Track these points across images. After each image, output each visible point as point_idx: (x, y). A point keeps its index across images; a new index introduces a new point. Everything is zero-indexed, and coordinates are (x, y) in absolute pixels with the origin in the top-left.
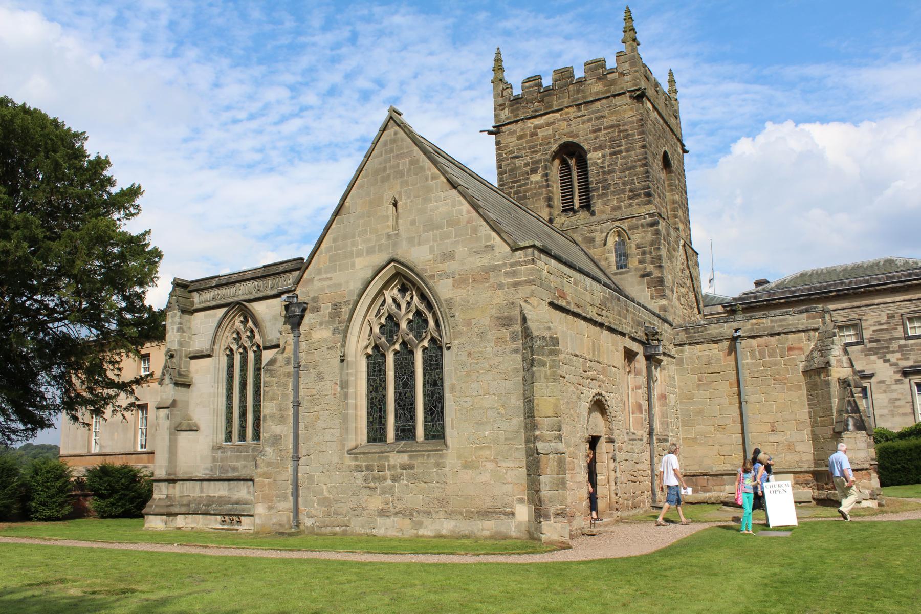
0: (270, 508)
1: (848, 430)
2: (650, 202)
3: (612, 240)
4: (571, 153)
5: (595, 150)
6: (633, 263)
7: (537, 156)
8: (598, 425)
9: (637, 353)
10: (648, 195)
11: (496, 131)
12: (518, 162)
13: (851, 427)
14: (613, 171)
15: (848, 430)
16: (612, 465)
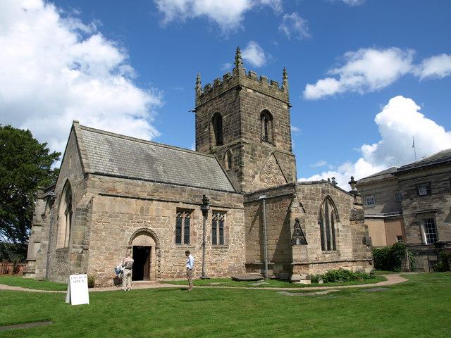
0: (40, 271)
1: (295, 244)
2: (241, 137)
3: (226, 157)
4: (217, 120)
5: (225, 115)
6: (233, 166)
7: (207, 120)
8: (141, 241)
9: (193, 210)
10: (240, 133)
11: (196, 110)
12: (202, 123)
13: (298, 243)
14: (229, 124)
15: (295, 244)
16: (158, 258)
